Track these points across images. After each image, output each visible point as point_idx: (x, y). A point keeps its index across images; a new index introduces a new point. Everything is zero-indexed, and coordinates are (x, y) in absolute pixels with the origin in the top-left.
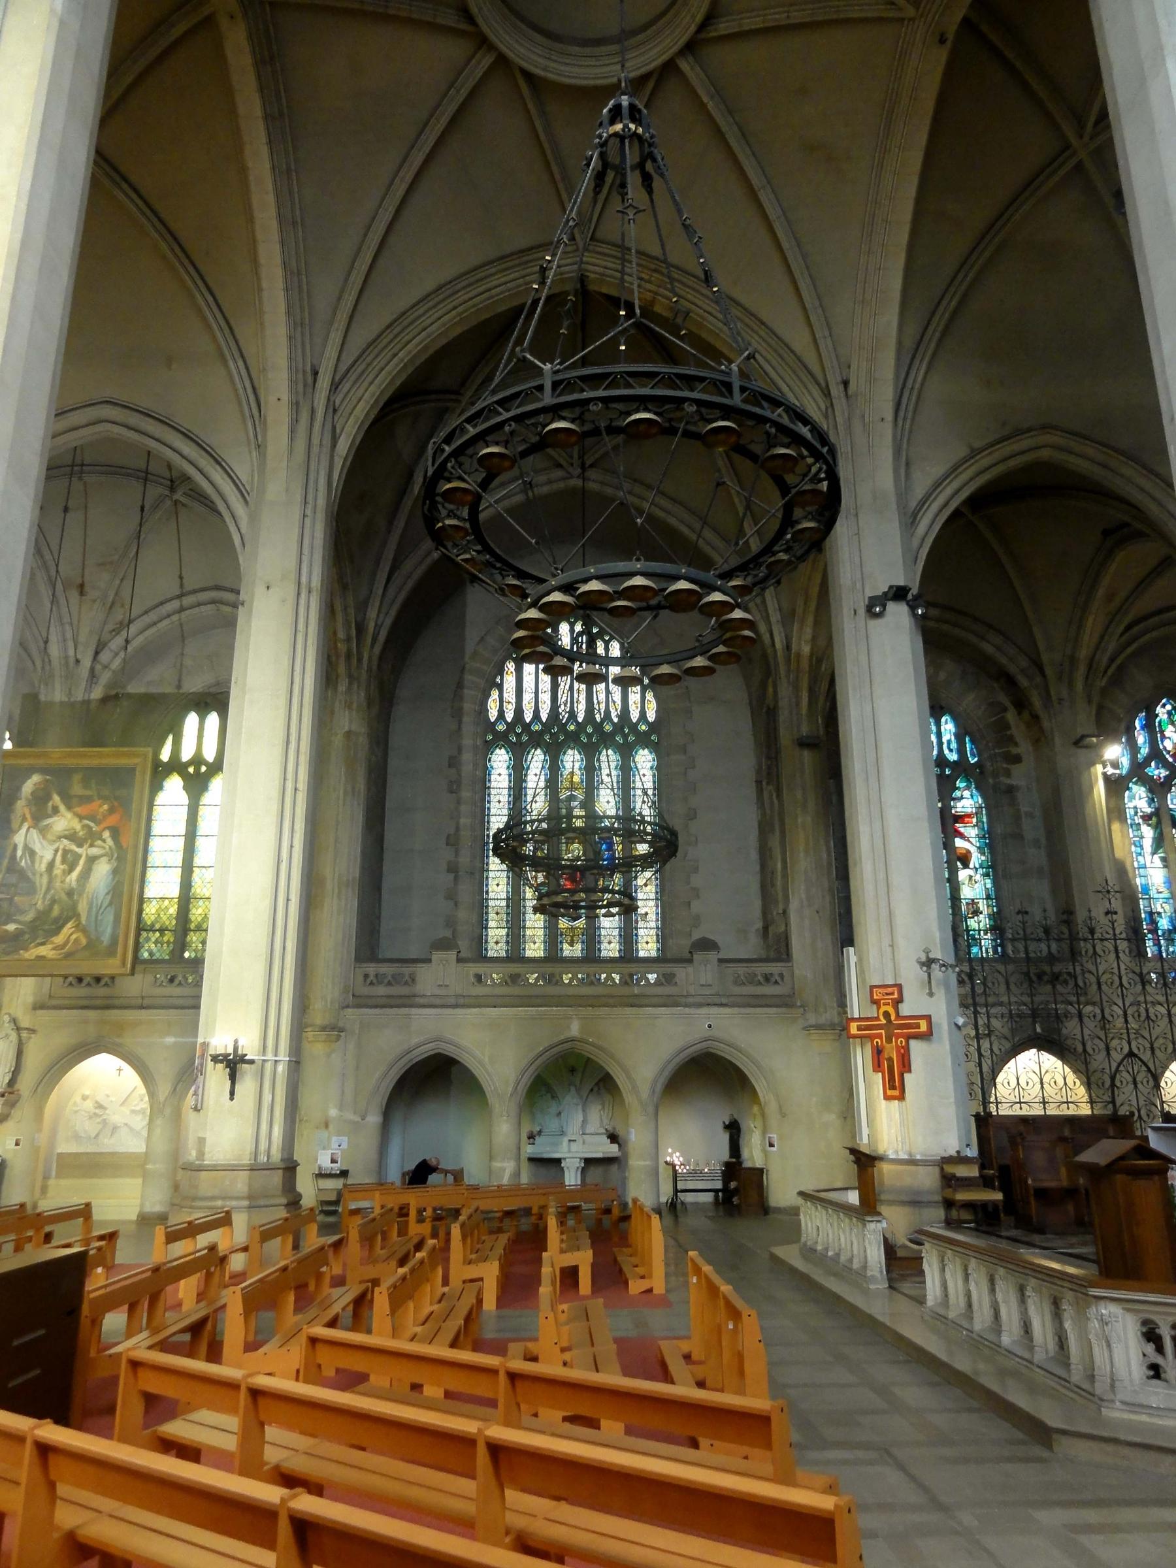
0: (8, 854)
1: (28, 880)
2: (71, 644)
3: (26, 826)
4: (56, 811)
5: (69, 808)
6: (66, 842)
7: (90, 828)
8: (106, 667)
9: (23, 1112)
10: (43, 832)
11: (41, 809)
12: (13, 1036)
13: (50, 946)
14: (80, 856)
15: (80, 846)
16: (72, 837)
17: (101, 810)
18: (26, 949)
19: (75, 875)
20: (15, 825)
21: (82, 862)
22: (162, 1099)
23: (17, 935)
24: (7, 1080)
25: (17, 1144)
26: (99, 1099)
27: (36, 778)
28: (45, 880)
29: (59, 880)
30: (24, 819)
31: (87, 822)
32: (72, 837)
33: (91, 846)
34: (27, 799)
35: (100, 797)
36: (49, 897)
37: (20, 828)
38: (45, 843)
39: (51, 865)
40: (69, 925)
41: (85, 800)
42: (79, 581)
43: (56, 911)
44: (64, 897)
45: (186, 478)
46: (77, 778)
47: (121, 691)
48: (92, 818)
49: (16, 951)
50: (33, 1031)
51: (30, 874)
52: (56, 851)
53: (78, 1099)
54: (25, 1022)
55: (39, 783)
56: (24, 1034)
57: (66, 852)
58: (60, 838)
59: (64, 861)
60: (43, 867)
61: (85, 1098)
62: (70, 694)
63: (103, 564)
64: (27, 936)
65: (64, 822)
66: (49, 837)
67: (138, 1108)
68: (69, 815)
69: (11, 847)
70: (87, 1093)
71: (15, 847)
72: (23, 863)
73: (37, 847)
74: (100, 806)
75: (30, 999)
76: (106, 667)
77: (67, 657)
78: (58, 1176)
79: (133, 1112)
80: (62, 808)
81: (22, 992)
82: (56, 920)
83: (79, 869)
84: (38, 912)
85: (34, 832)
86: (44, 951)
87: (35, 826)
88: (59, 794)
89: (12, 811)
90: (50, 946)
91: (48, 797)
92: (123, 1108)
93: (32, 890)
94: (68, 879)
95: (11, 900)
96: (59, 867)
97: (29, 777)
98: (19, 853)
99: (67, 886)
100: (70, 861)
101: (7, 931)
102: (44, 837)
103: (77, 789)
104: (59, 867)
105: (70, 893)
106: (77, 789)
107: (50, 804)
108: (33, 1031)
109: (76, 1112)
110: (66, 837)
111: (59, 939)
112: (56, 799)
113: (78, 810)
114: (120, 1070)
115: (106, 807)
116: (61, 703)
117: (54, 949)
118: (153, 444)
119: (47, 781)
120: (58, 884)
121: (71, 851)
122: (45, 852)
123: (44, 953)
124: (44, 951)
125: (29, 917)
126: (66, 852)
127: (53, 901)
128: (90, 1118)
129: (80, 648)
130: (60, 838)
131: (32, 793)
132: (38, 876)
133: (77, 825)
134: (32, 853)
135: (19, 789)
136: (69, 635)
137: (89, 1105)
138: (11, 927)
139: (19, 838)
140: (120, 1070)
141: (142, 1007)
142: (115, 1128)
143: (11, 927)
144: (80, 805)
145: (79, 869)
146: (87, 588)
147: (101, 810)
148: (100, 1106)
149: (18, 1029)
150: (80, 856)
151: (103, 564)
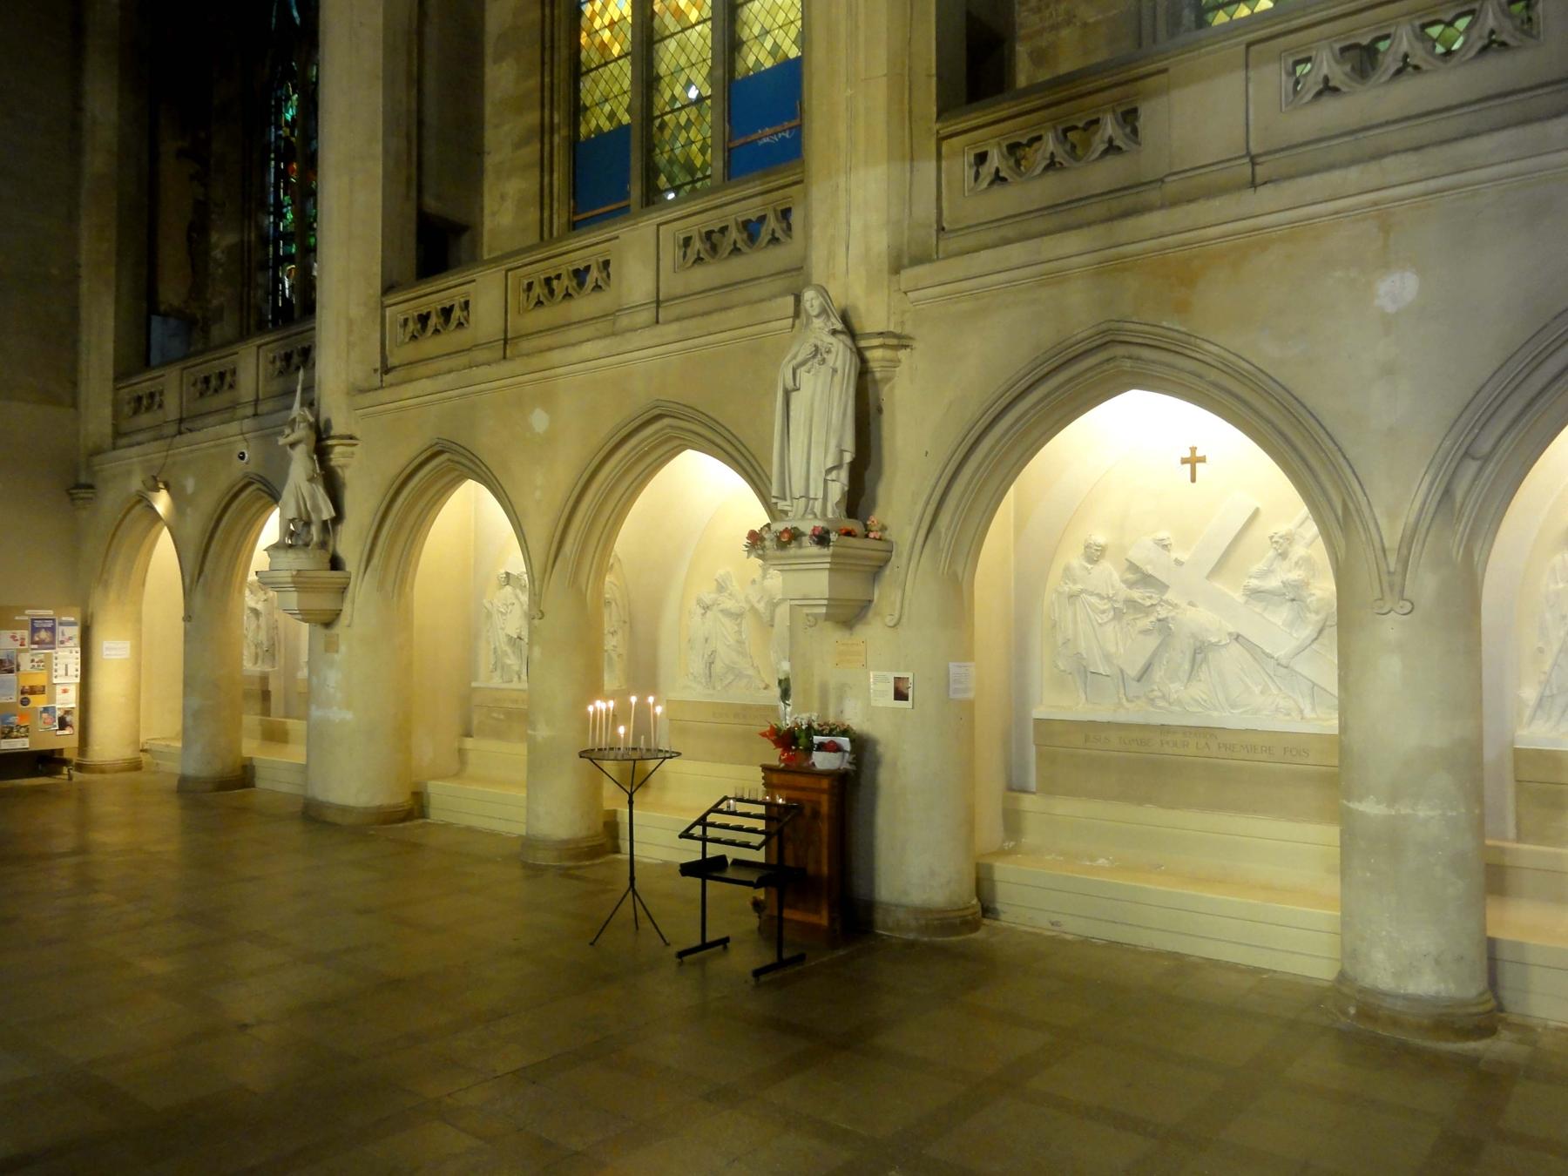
9: (908, 590)
12: (840, 354)
22: (1391, 535)
24: (837, 489)
25: (900, 695)
26: (1136, 555)
50: (900, 341)
53: (1076, 561)
54: (875, 316)
56: (875, 356)
61: (1094, 554)
67: (1273, 583)
70: (1100, 538)
75: (880, 242)
78: (1050, 788)
79: (1255, 594)
81: (857, 225)
92: (1218, 585)
108: (900, 341)
109: (1072, 597)
114: (1193, 461)
128: (1118, 615)
137: (1108, 575)
140: (1193, 461)
141: (1253, 184)
142: (1200, 651)
148: (1144, 579)
149: (849, 328)
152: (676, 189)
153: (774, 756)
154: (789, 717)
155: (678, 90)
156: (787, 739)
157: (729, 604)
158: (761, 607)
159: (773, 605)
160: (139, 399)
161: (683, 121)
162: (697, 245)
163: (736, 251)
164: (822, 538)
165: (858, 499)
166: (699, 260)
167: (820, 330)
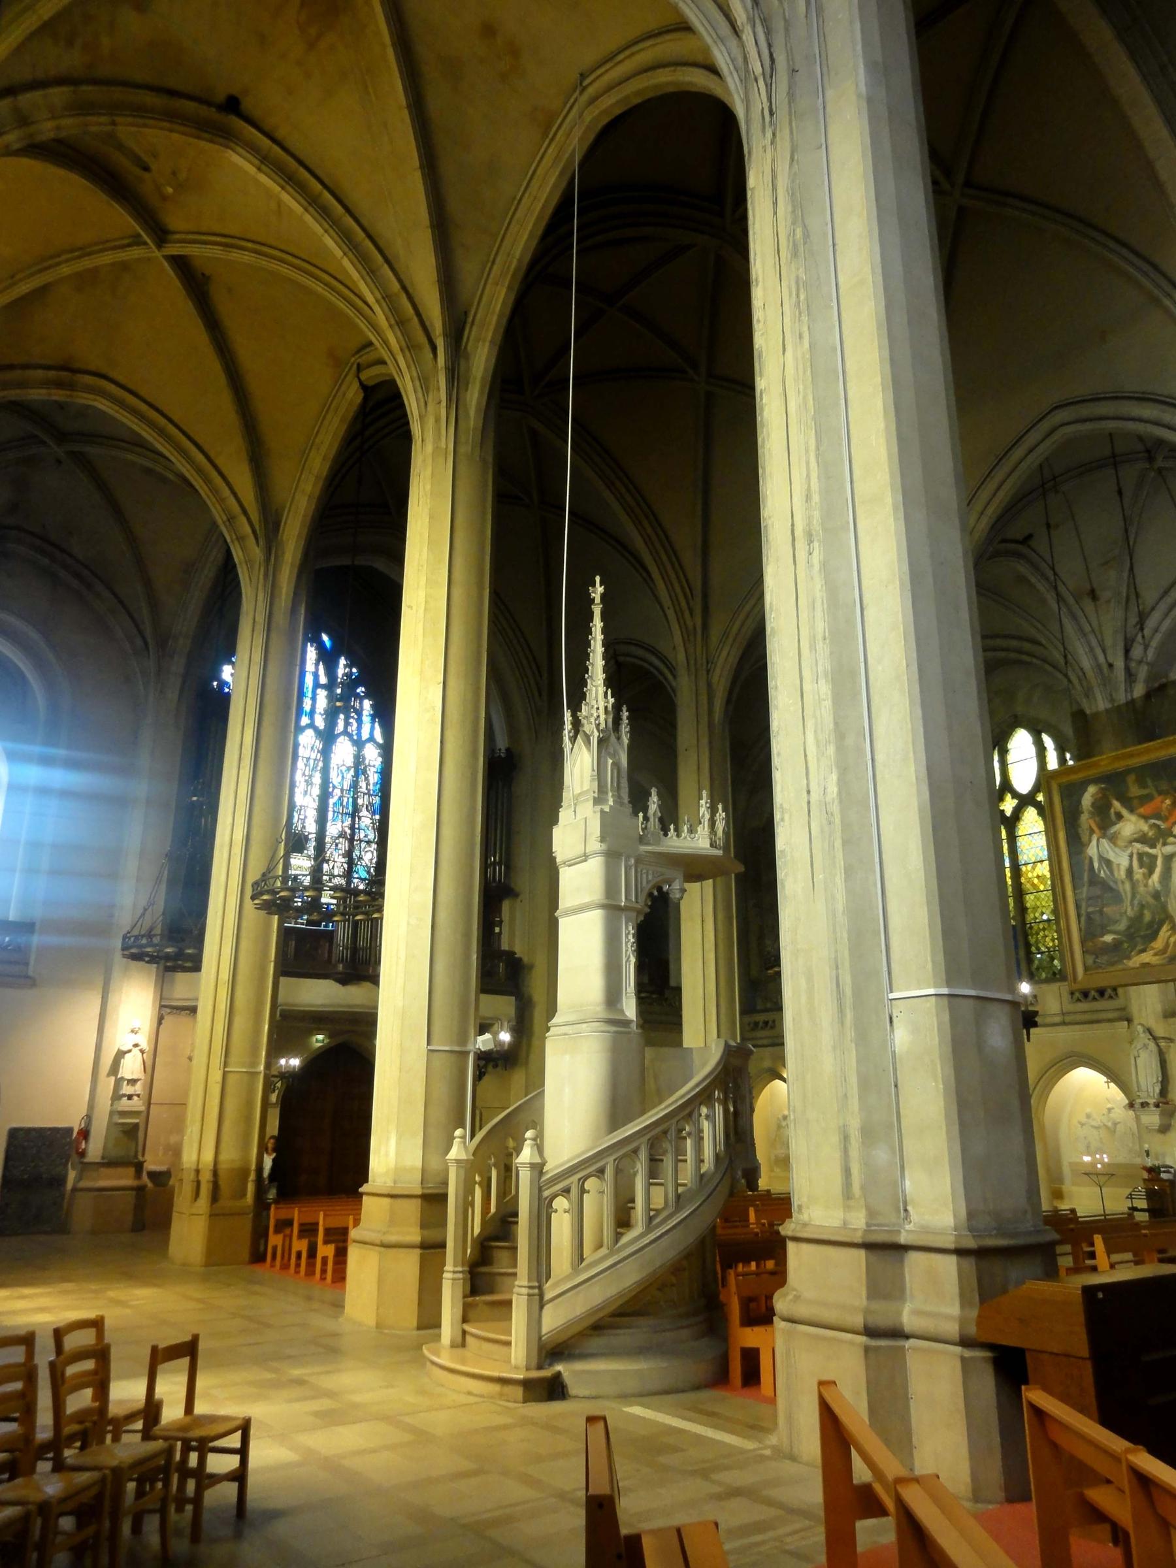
0: (1086, 867)
1: (1111, 889)
2: (1098, 651)
3: (1095, 838)
4: (1120, 817)
5: (1132, 810)
6: (1138, 845)
7: (1158, 827)
8: (1140, 662)
10: (1113, 839)
11: (1105, 819)
12: (1152, 1045)
13: (1152, 952)
14: (1155, 857)
15: (1153, 846)
16: (1142, 839)
17: (1164, 806)
18: (1129, 958)
19: (1156, 877)
20: (1085, 838)
21: (1159, 862)
23: (1116, 946)
24: (1157, 1090)
27: (1092, 790)
28: (1128, 886)
29: (1141, 884)
30: (1092, 832)
31: (1153, 821)
32: (1142, 839)
33: (1165, 844)
34: (1090, 812)
35: (1160, 793)
36: (1136, 902)
37: (1090, 841)
38: (1117, 850)
39: (1130, 872)
40: (1165, 928)
41: (1145, 799)
42: (1089, 587)
43: (1148, 916)
44: (1150, 900)
45: (1160, 442)
46: (1131, 779)
47: (1164, 680)
48: (1158, 816)
49: (1119, 961)
50: (1171, 1040)
51: (1112, 884)
52: (1131, 856)
54: (1160, 1031)
55: (1097, 793)
56: (1163, 1044)
57: (1141, 856)
58: (1131, 842)
59: (1141, 866)
60: (1123, 874)
62: (1112, 700)
63: (1106, 563)
64: (1126, 945)
65: (1130, 825)
66: (1121, 843)
68: (1133, 818)
69: (1087, 861)
71: (1091, 859)
72: (1102, 874)
73: (1111, 856)
74: (1162, 802)
75: (1159, 1008)
76: (1140, 662)
77: (1099, 666)
80: (1124, 812)
82: (1150, 924)
83: (1158, 870)
84: (1130, 919)
85: (1104, 841)
86: (1147, 957)
87: (1104, 836)
88: (1117, 799)
89: (1079, 826)
90: (1152, 952)
91: (1109, 806)
93: (1117, 898)
94: (1150, 882)
95: (1101, 912)
96: (1139, 873)
97: (1085, 790)
98: (1096, 865)
99: (1151, 889)
100: (1148, 863)
101: (1104, 942)
102: (1115, 844)
103: (1134, 790)
104: (1139, 873)
105: (1156, 895)
106: (1134, 790)
107: (1112, 810)
110: (1136, 841)
111: (1158, 944)
112: (1117, 804)
113: (1142, 810)
115: (1168, 802)
116: (1107, 711)
117: (1155, 954)
118: (1111, 425)
119: (1102, 789)
120: (1142, 889)
121: (1148, 854)
122: (1121, 860)
123: (1147, 960)
124: (1147, 957)
125: (1122, 926)
126: (1141, 856)
127: (1142, 907)
129: (1109, 652)
130: (1131, 842)
131: (1093, 805)
132: (1120, 885)
133: (1145, 827)
134: (1108, 863)
135: (1079, 802)
136: (1094, 642)
138: (1108, 938)
139: (1092, 851)
143: (1108, 938)
144: (1142, 805)
145: (1158, 870)
146: (1098, 592)
147: (1164, 806)
149: (1155, 1038)
150: (1155, 857)
151: (1106, 563)
152: (1042, 953)
153: (1145, 1175)
154: (1149, 1163)
155: (1037, 915)
156: (1150, 1170)
157: (1094, 1123)
158: (1110, 1124)
159: (1115, 1124)
160: (756, 1024)
161: (1041, 926)
162: (1077, 995)
163: (1094, 999)
164: (1157, 1106)
165: (1164, 1092)
166: (1079, 1000)
167: (1144, 1038)
